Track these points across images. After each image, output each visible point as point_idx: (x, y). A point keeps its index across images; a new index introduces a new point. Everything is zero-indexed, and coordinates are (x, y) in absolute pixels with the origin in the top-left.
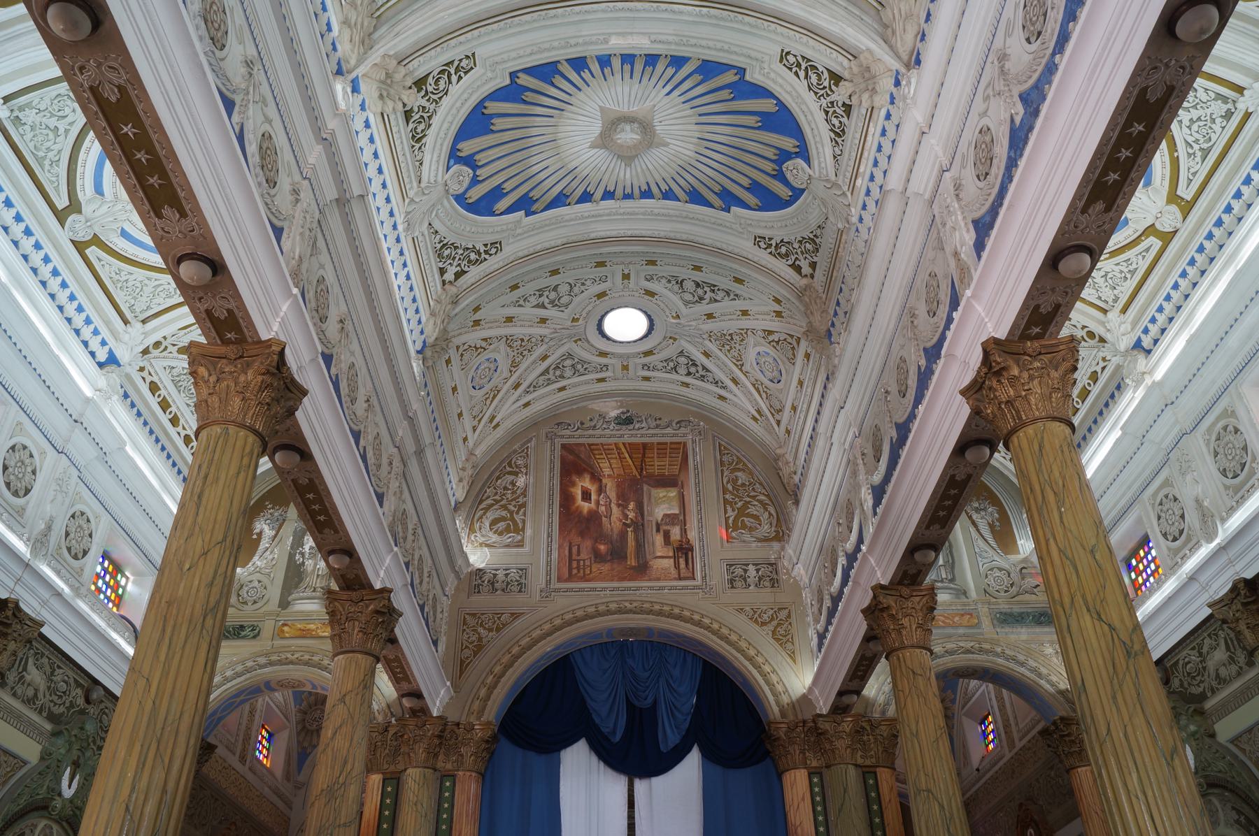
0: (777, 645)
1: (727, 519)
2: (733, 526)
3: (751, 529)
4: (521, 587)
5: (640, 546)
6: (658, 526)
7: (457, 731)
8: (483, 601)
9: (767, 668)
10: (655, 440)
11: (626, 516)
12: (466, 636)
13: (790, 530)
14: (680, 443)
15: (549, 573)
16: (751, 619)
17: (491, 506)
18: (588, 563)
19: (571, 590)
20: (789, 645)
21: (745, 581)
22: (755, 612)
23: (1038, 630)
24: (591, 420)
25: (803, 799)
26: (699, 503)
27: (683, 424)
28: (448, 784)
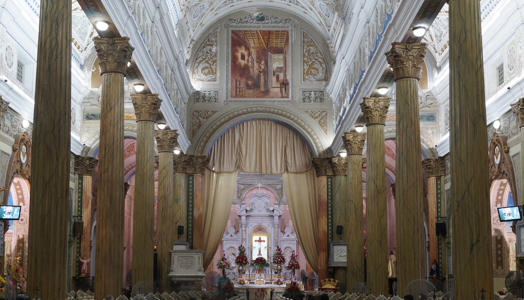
0: (320, 127)
1: (304, 70)
2: (306, 74)
3: (314, 75)
4: (216, 100)
5: (266, 82)
6: (274, 72)
7: (193, 159)
8: (200, 106)
9: (315, 137)
10: (275, 29)
11: (260, 67)
12: (194, 121)
13: (331, 75)
14: (286, 31)
15: (227, 94)
16: (311, 116)
17: (202, 61)
18: (244, 89)
19: (237, 101)
20: (325, 127)
21: (310, 99)
22: (312, 113)
23: (428, 123)
24: (245, 18)
25: (324, 187)
26: (292, 62)
27: (287, 21)
28: (191, 178)
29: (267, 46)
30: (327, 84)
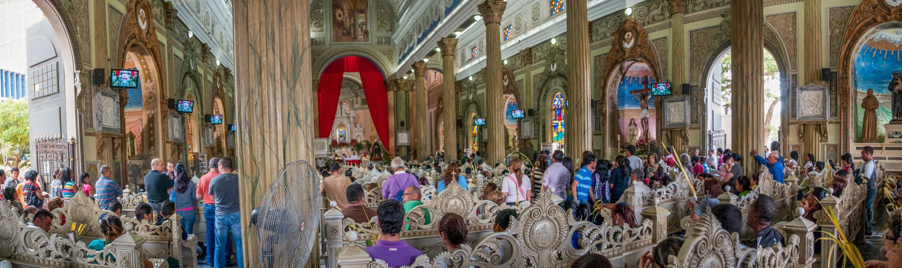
2: (380, 26)
3: (384, 28)
15: (331, 39)
30: (392, 34)
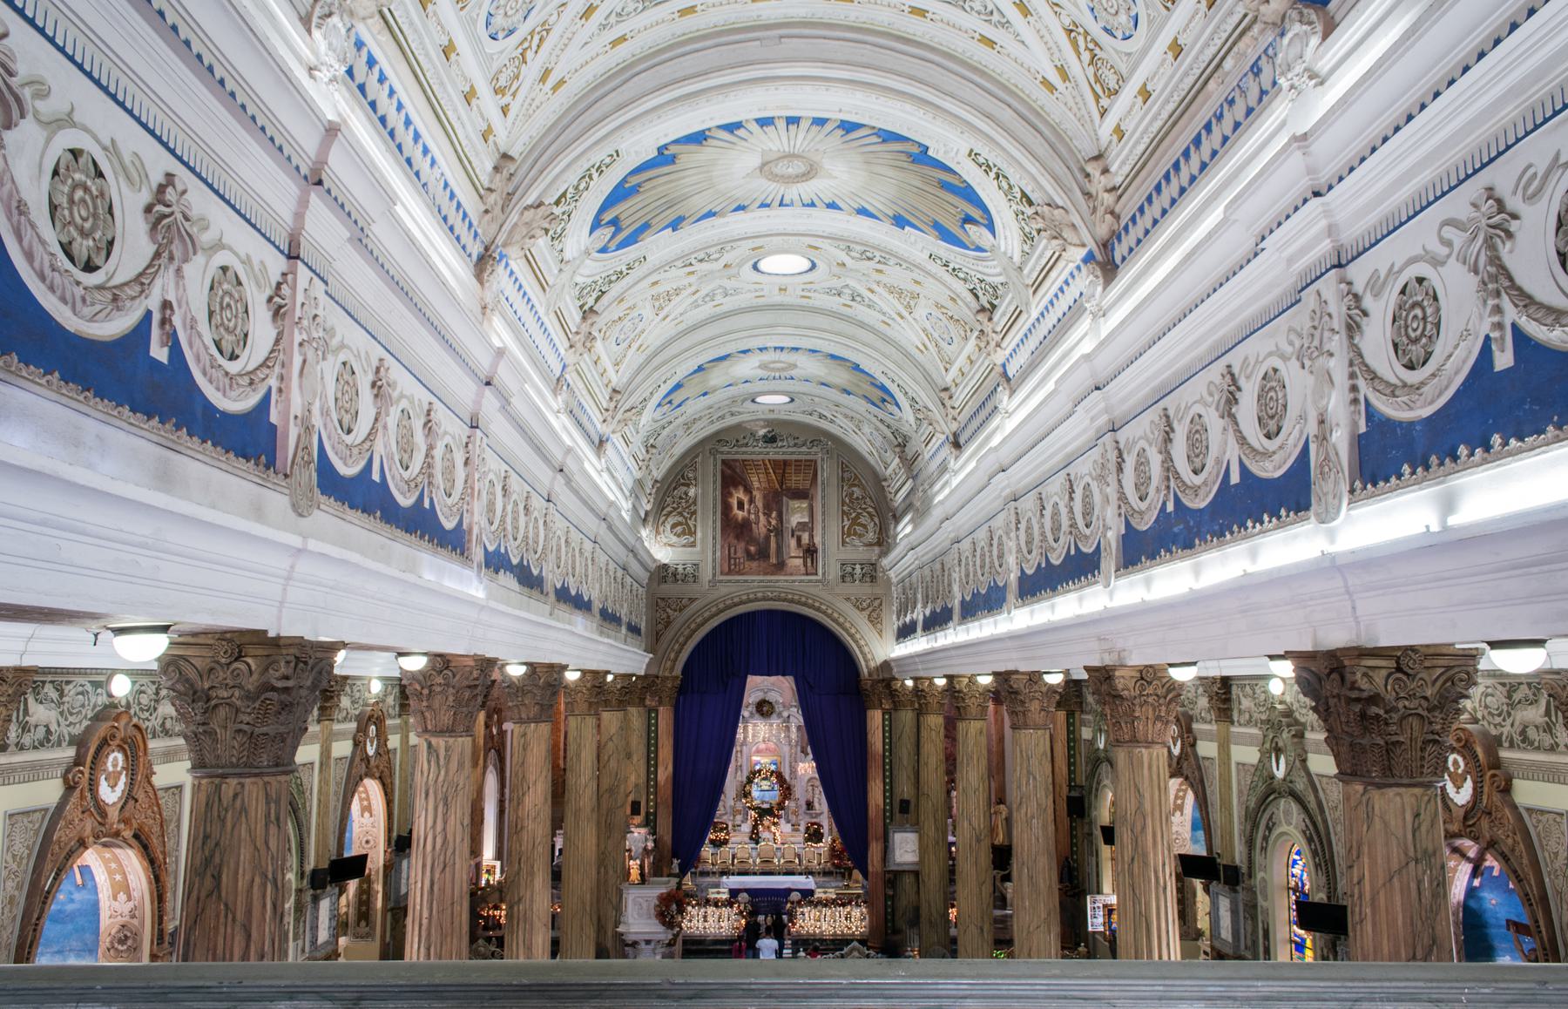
2: (847, 534)
3: (860, 536)
8: (669, 589)
9: (862, 642)
10: (794, 457)
11: (770, 523)
15: (714, 568)
17: (671, 512)
19: (730, 581)
26: (823, 513)
29: (781, 484)
30: (884, 554)
